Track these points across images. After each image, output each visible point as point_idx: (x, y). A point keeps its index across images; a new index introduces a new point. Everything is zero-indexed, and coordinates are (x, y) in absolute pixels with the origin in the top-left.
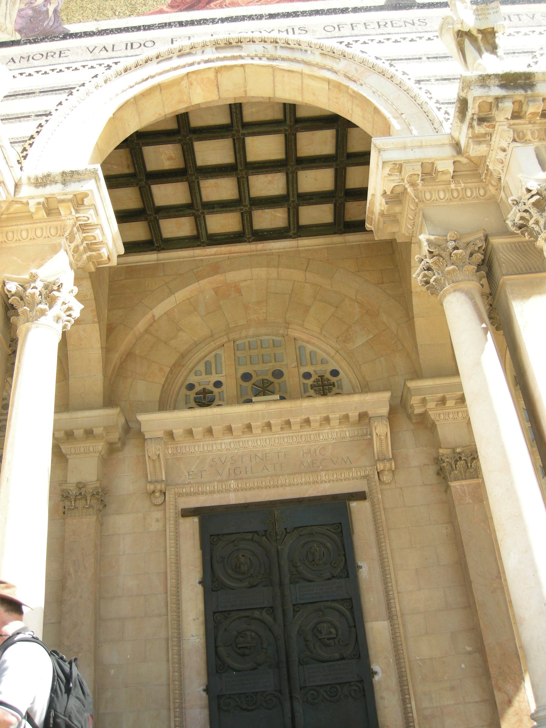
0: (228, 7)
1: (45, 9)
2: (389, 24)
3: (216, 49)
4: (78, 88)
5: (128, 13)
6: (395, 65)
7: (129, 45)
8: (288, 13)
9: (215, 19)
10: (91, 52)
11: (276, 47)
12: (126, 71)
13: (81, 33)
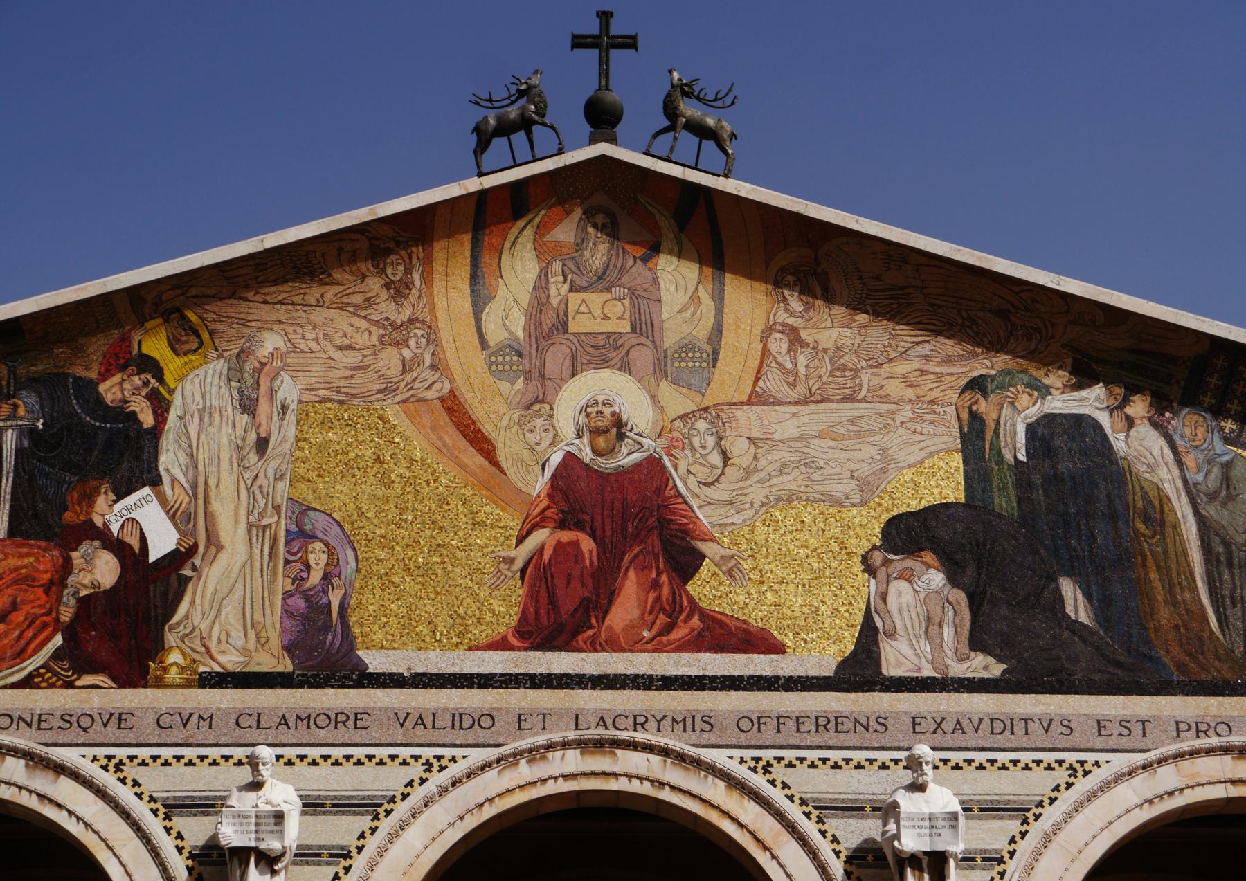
0: (604, 650)
1: (324, 600)
2: (831, 726)
3: (582, 754)
5: (455, 640)
6: (825, 820)
7: (457, 715)
8: (690, 677)
9: (585, 675)
10: (402, 725)
11: (665, 761)
13: (384, 674)
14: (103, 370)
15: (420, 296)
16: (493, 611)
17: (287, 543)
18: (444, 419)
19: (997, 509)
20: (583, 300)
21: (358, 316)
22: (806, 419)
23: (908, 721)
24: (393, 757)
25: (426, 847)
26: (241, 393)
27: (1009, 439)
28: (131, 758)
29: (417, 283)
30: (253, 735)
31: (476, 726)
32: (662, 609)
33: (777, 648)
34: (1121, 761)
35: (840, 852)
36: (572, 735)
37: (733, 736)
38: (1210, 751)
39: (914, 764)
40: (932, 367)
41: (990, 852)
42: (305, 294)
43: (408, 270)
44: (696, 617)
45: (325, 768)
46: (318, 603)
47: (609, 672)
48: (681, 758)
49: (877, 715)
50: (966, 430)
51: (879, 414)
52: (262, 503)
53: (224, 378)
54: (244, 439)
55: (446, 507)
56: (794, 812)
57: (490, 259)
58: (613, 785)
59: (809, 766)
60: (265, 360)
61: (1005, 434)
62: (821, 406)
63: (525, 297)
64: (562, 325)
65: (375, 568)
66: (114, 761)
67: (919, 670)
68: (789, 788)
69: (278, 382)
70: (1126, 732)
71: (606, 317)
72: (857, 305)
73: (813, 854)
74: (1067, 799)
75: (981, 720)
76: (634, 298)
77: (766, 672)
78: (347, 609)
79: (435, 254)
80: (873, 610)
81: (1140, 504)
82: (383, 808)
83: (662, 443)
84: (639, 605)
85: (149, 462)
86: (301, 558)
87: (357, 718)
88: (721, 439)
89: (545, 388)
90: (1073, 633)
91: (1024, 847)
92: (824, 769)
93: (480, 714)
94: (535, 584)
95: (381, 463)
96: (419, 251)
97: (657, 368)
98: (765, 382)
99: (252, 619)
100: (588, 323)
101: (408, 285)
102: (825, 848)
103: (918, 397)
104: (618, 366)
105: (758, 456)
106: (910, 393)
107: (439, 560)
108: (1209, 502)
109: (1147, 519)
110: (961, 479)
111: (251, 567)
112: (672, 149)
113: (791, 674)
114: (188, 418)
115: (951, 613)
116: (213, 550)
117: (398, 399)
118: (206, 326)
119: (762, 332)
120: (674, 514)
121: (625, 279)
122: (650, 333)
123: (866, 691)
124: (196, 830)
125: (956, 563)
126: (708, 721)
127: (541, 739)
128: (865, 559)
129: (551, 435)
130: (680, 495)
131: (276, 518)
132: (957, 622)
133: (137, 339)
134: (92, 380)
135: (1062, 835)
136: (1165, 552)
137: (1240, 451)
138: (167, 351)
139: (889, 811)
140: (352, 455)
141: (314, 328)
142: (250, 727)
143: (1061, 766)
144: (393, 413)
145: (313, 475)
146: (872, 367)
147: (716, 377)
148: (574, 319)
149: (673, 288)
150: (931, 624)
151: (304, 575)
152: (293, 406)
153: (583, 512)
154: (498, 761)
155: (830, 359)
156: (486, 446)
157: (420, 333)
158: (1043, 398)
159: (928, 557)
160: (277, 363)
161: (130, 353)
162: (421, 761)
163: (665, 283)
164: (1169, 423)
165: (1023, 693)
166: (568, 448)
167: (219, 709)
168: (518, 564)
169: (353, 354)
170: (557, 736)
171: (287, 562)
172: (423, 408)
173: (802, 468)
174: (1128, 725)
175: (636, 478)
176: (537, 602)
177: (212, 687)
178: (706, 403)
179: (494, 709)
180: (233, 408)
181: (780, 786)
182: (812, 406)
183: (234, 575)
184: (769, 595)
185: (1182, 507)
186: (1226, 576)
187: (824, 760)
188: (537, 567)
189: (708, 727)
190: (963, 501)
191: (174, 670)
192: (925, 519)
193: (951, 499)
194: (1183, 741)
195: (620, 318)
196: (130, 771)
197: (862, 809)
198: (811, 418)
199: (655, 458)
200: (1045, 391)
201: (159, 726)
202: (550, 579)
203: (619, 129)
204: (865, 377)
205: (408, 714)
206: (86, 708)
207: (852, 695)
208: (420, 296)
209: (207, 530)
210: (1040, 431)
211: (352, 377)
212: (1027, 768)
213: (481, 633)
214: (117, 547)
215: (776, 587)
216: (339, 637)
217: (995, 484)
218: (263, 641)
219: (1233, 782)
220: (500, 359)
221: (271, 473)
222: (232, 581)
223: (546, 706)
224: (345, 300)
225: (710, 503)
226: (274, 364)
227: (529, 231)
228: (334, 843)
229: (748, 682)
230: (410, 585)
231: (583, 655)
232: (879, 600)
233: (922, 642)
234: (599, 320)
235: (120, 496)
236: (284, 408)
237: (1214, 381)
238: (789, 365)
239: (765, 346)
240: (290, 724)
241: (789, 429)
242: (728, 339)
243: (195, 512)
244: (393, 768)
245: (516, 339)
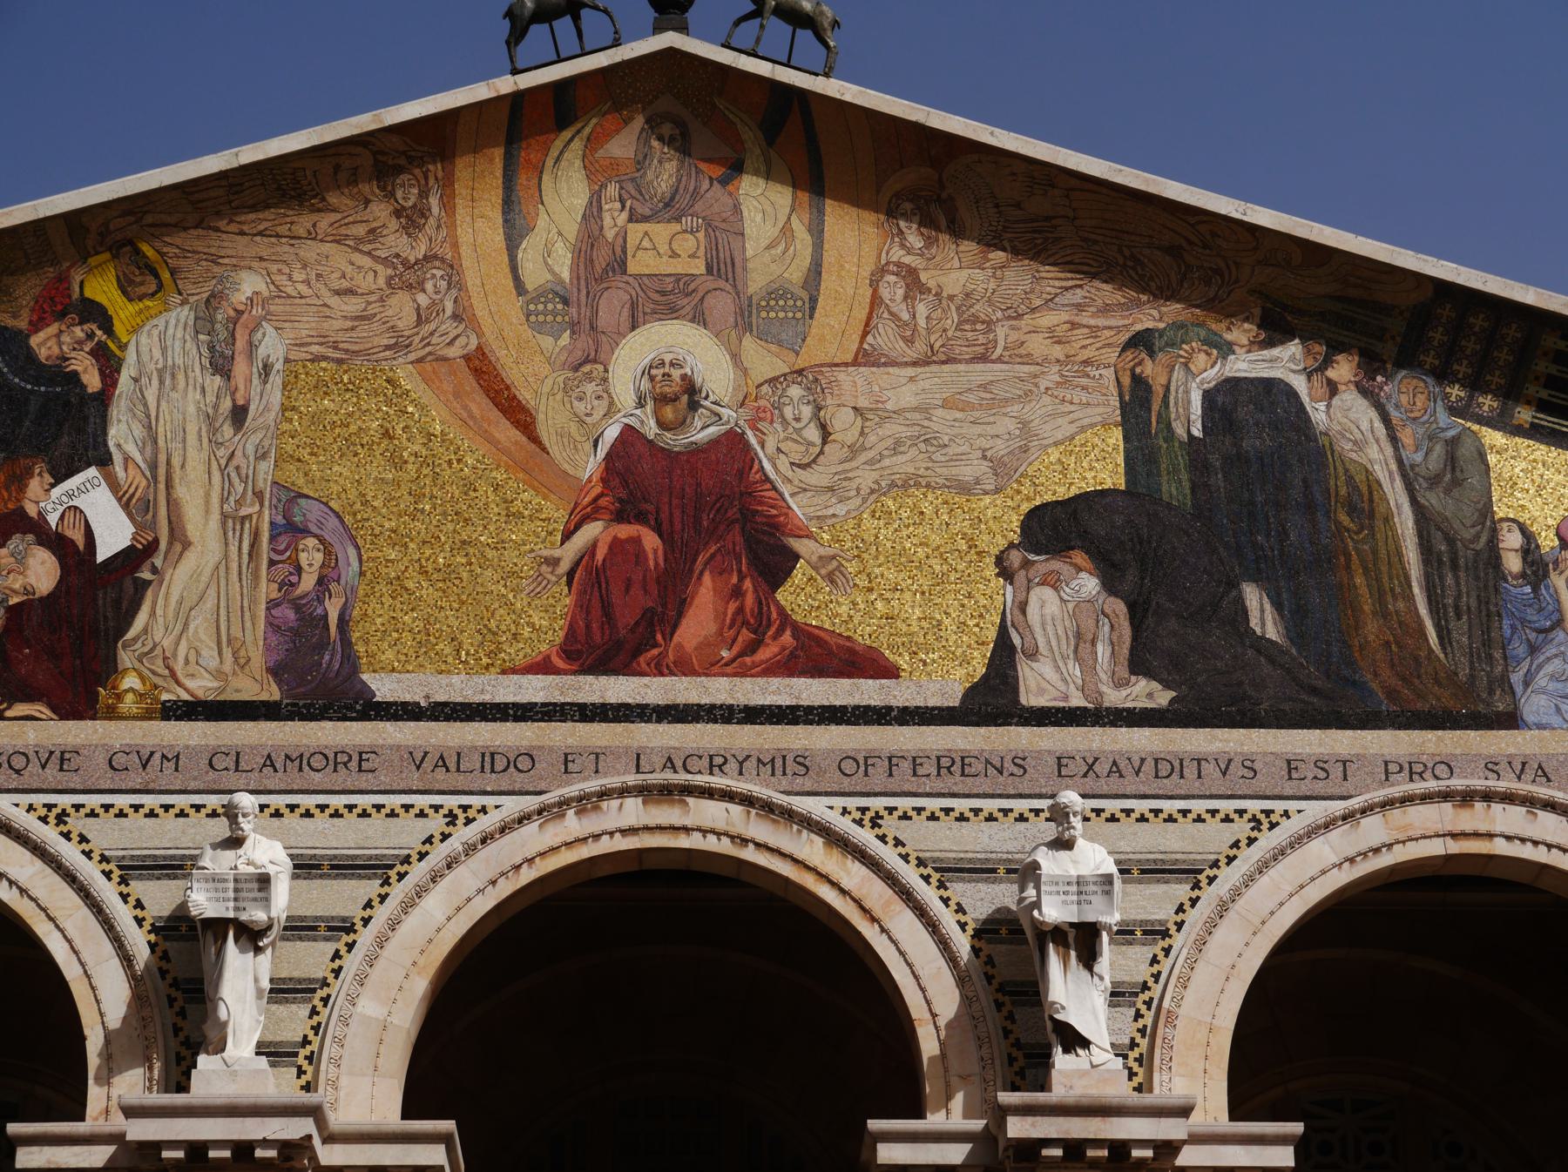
0: (672, 674)
1: (319, 611)
2: (956, 769)
3: (644, 803)
4: (399, 868)
5: (485, 661)
6: (948, 884)
7: (487, 755)
8: (780, 707)
9: (647, 705)
10: (418, 768)
11: (749, 812)
12: (484, 841)
13: (395, 703)
14: (35, 318)
15: (439, 227)
16: (532, 625)
17: (272, 538)
18: (470, 383)
19: (1165, 497)
20: (646, 233)
21: (361, 251)
22: (926, 384)
23: (1052, 761)
24: (407, 807)
25: (449, 919)
26: (211, 348)
27: (1181, 410)
28: (77, 807)
29: (435, 210)
30: (230, 780)
31: (512, 769)
32: (745, 623)
33: (891, 672)
34: (1316, 811)
35: (966, 924)
36: (632, 779)
37: (834, 780)
38: (1426, 798)
39: (1059, 815)
40: (1085, 319)
41: (1152, 923)
42: (292, 223)
43: (424, 194)
44: (788, 633)
45: (321, 821)
46: (311, 614)
47: (678, 701)
48: (768, 809)
49: (1013, 754)
50: (1127, 398)
51: (1018, 378)
52: (240, 489)
53: (190, 330)
54: (216, 407)
55: (473, 494)
56: (910, 875)
57: (528, 180)
58: (683, 842)
59: (928, 819)
60: (242, 307)
61: (1176, 404)
62: (946, 368)
63: (572, 229)
64: (623, 265)
65: (384, 571)
66: (55, 811)
67: (1066, 698)
68: (904, 845)
69: (259, 335)
70: (1322, 775)
71: (674, 255)
72: (992, 241)
73: (932, 926)
74: (1249, 858)
75: (1143, 760)
76: (710, 230)
77: (876, 700)
78: (348, 622)
79: (458, 174)
80: (1009, 623)
81: (1343, 491)
82: (396, 870)
84: (716, 617)
85: (95, 436)
86: (289, 558)
87: (362, 759)
88: (819, 409)
89: (597, 344)
90: (1259, 652)
91: (1194, 917)
92: (946, 822)
93: (517, 753)
94: (585, 591)
95: (391, 438)
96: (436, 169)
97: (739, 319)
98: (875, 338)
99: (228, 635)
100: (652, 263)
101: (424, 213)
102: (948, 920)
103: (1067, 357)
104: (690, 316)
105: (866, 431)
106: (1058, 352)
107: (464, 561)
108: (1430, 488)
109: (1352, 510)
110: (1121, 460)
111: (227, 568)
112: (758, 40)
113: (907, 704)
114: (144, 380)
115: (1107, 628)
116: (178, 547)
117: (412, 357)
118: (167, 264)
119: (872, 275)
120: (761, 503)
121: (698, 207)
122: (730, 275)
123: (1000, 725)
124: (160, 897)
125: (1113, 565)
126: (803, 762)
127: (593, 785)
128: (999, 560)
129: (605, 403)
130: (767, 479)
131: (257, 508)
132: (1115, 639)
133: (78, 279)
134: (21, 331)
135: (1241, 903)
136: (1375, 552)
137: (1469, 424)
138: (116, 294)
139: (1028, 873)
140: (353, 428)
141: (305, 267)
142: (226, 769)
143: (1241, 817)
144: (406, 375)
145: (304, 453)
146: (1010, 318)
147: (814, 331)
148: (634, 256)
149: (759, 217)
150: (1082, 641)
151: (294, 579)
152: (279, 366)
153: (646, 502)
154: (540, 812)
155: (958, 309)
156: (523, 417)
157: (439, 273)
158: (1225, 358)
159: (1079, 557)
160: (257, 311)
161: (70, 297)
162: (442, 812)
163: (750, 211)
164: (1381, 389)
165: (1196, 727)
166: (626, 420)
167: (187, 747)
168: (564, 566)
169: (354, 300)
170: (613, 781)
171: (272, 563)
172: (443, 369)
173: (922, 446)
174: (1325, 766)
175: (713, 457)
176: (588, 613)
177: (178, 719)
178: (800, 364)
179: (534, 747)
180: (202, 367)
181: (891, 842)
182: (934, 368)
183: (204, 579)
184: (879, 605)
185: (1396, 494)
186: (1449, 580)
187: (947, 811)
188: (588, 570)
189: (802, 770)
190: (1123, 487)
191: (129, 697)
192: (1075, 511)
193: (1108, 485)
194: (1393, 785)
195: (693, 256)
196: (76, 824)
197: (994, 871)
198: (935, 381)
199: (736, 434)
200: (1226, 349)
201: (112, 767)
202: (604, 586)
203: (692, 15)
204: (1001, 332)
205: (426, 753)
206: (19, 744)
207: (983, 730)
208: (439, 227)
209: (170, 522)
210: (1220, 399)
211: (353, 329)
212: (1199, 819)
213: (516, 653)
214: (56, 543)
215: (888, 595)
216: (339, 657)
218: (242, 661)
219: (1454, 836)
220: (541, 307)
221: (250, 449)
222: (202, 586)
223: (599, 743)
224: (343, 231)
225: (805, 490)
226: (254, 312)
227: (577, 145)
228: (334, 914)
229: (853, 714)
230: (427, 592)
231: (646, 680)
232: (1017, 612)
233: (1071, 663)
234: (665, 258)
235: (59, 479)
236: (267, 368)
237: (1438, 336)
238: (905, 316)
239: (875, 291)
240: (278, 766)
241: (906, 397)
242: (828, 282)
243: (155, 499)
244: (407, 820)
245: (561, 282)
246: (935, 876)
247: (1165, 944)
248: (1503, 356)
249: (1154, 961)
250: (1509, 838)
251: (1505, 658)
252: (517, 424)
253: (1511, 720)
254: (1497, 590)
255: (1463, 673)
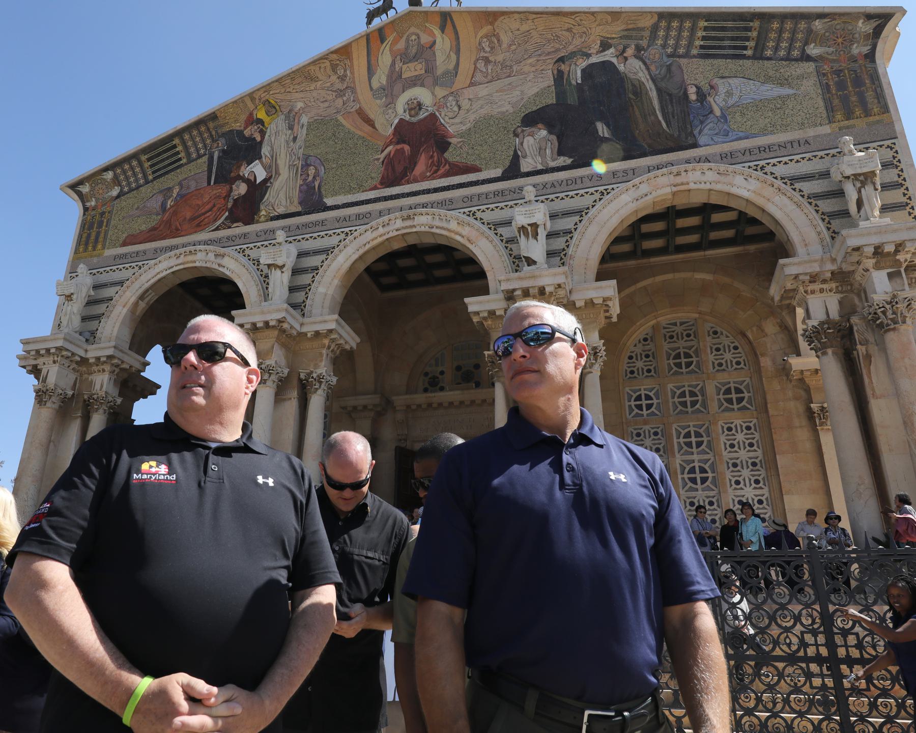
18: (356, 117)
19: (569, 103)
40: (542, 58)
43: (345, 71)
58: (414, 230)
64: (401, 76)
74: (599, 205)
81: (631, 88)
83: (435, 108)
87: (323, 222)
91: (580, 226)
96: (348, 62)
106: (533, 69)
126: (451, 201)
128: (514, 131)
129: (394, 114)
150: (541, 151)
159: (540, 126)
160: (301, 112)
168: (381, 160)
171: (301, 175)
185: (650, 85)
186: (670, 107)
196: (247, 252)
200: (588, 56)
204: (514, 68)
206: (234, 234)
217: (568, 94)
236: (303, 125)
238: (485, 70)
246: (493, 227)
247: (571, 235)
248: (686, 34)
249: (567, 241)
250: (695, 183)
251: (691, 127)
252: (369, 125)
253: (695, 145)
254: (687, 107)
255: (676, 135)
